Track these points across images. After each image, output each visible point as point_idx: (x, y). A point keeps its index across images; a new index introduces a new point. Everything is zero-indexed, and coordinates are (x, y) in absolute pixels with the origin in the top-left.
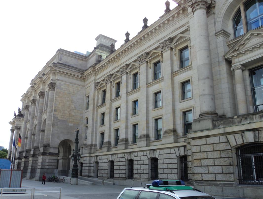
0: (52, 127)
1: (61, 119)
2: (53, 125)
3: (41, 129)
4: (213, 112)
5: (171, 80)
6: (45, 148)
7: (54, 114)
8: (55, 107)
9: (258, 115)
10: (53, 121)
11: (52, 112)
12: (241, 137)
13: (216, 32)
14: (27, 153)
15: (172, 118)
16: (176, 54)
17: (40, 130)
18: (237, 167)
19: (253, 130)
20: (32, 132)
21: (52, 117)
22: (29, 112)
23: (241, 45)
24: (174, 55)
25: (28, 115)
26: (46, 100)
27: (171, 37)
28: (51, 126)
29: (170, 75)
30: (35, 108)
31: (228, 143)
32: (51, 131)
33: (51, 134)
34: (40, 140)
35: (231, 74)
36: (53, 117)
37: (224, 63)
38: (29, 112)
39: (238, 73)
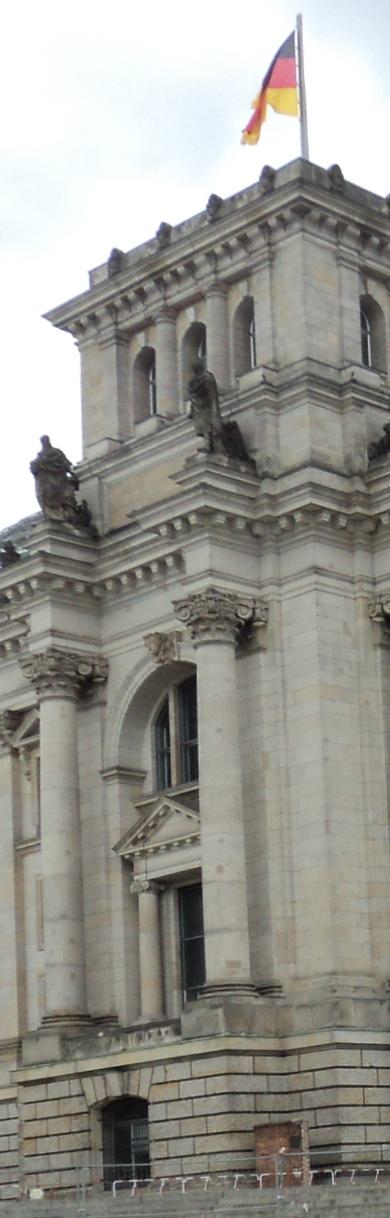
4: (72, 1013)
5: (10, 871)
9: (135, 1034)
12: (102, 1083)
13: (105, 767)
15: (15, 1000)
16: (28, 774)
18: (101, 1153)
19: (120, 1069)
23: (146, 829)
24: (24, 778)
27: (13, 709)
29: (10, 851)
31: (81, 1098)
35: (134, 899)
37: (118, 866)
39: (147, 901)
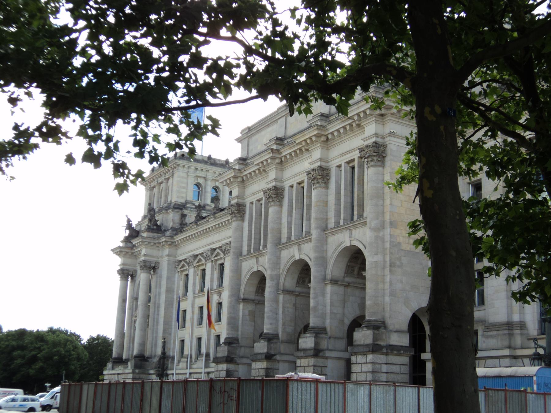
0: (390, 271)
1: (408, 249)
2: (390, 266)
3: (329, 277)
6: (376, 332)
7: (390, 235)
8: (392, 213)
10: (391, 253)
11: (383, 227)
14: (272, 345)
17: (325, 279)
20: (278, 284)
21: (383, 242)
22: (246, 224)
25: (242, 232)
26: (338, 193)
28: (384, 268)
30: (280, 212)
32: (388, 284)
33: (387, 292)
34: (328, 307)
36: (390, 241)
38: (246, 224)
